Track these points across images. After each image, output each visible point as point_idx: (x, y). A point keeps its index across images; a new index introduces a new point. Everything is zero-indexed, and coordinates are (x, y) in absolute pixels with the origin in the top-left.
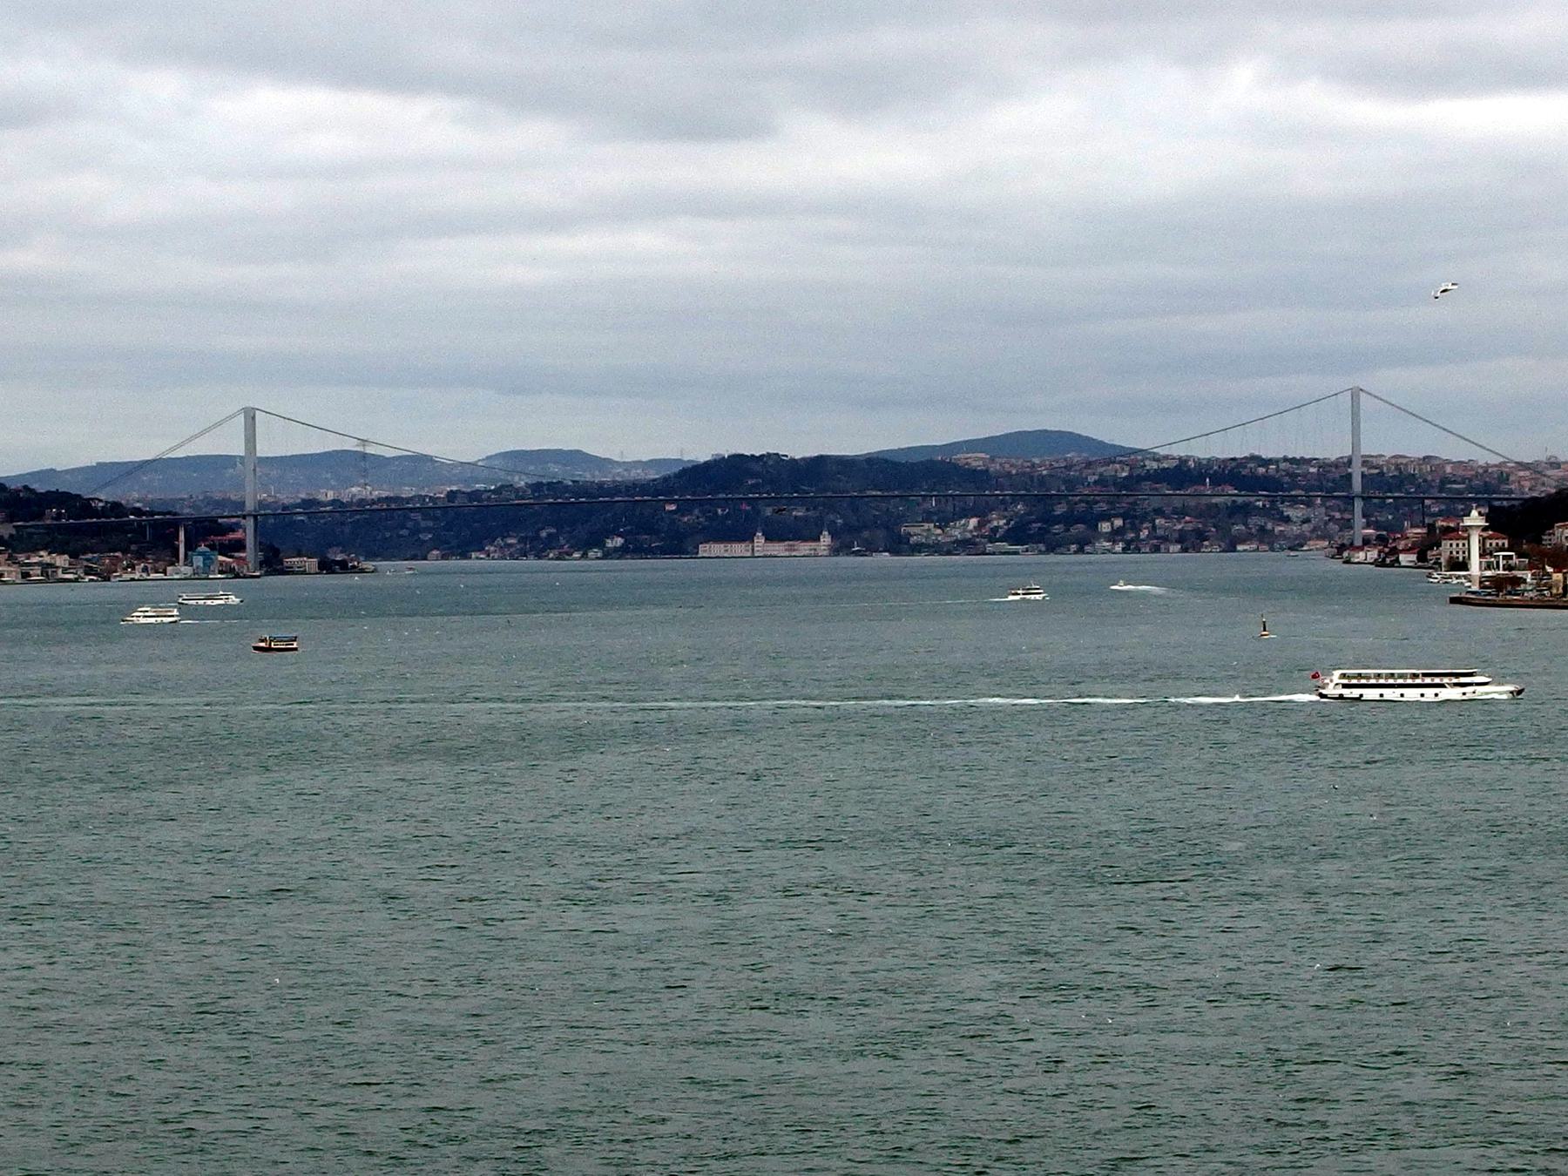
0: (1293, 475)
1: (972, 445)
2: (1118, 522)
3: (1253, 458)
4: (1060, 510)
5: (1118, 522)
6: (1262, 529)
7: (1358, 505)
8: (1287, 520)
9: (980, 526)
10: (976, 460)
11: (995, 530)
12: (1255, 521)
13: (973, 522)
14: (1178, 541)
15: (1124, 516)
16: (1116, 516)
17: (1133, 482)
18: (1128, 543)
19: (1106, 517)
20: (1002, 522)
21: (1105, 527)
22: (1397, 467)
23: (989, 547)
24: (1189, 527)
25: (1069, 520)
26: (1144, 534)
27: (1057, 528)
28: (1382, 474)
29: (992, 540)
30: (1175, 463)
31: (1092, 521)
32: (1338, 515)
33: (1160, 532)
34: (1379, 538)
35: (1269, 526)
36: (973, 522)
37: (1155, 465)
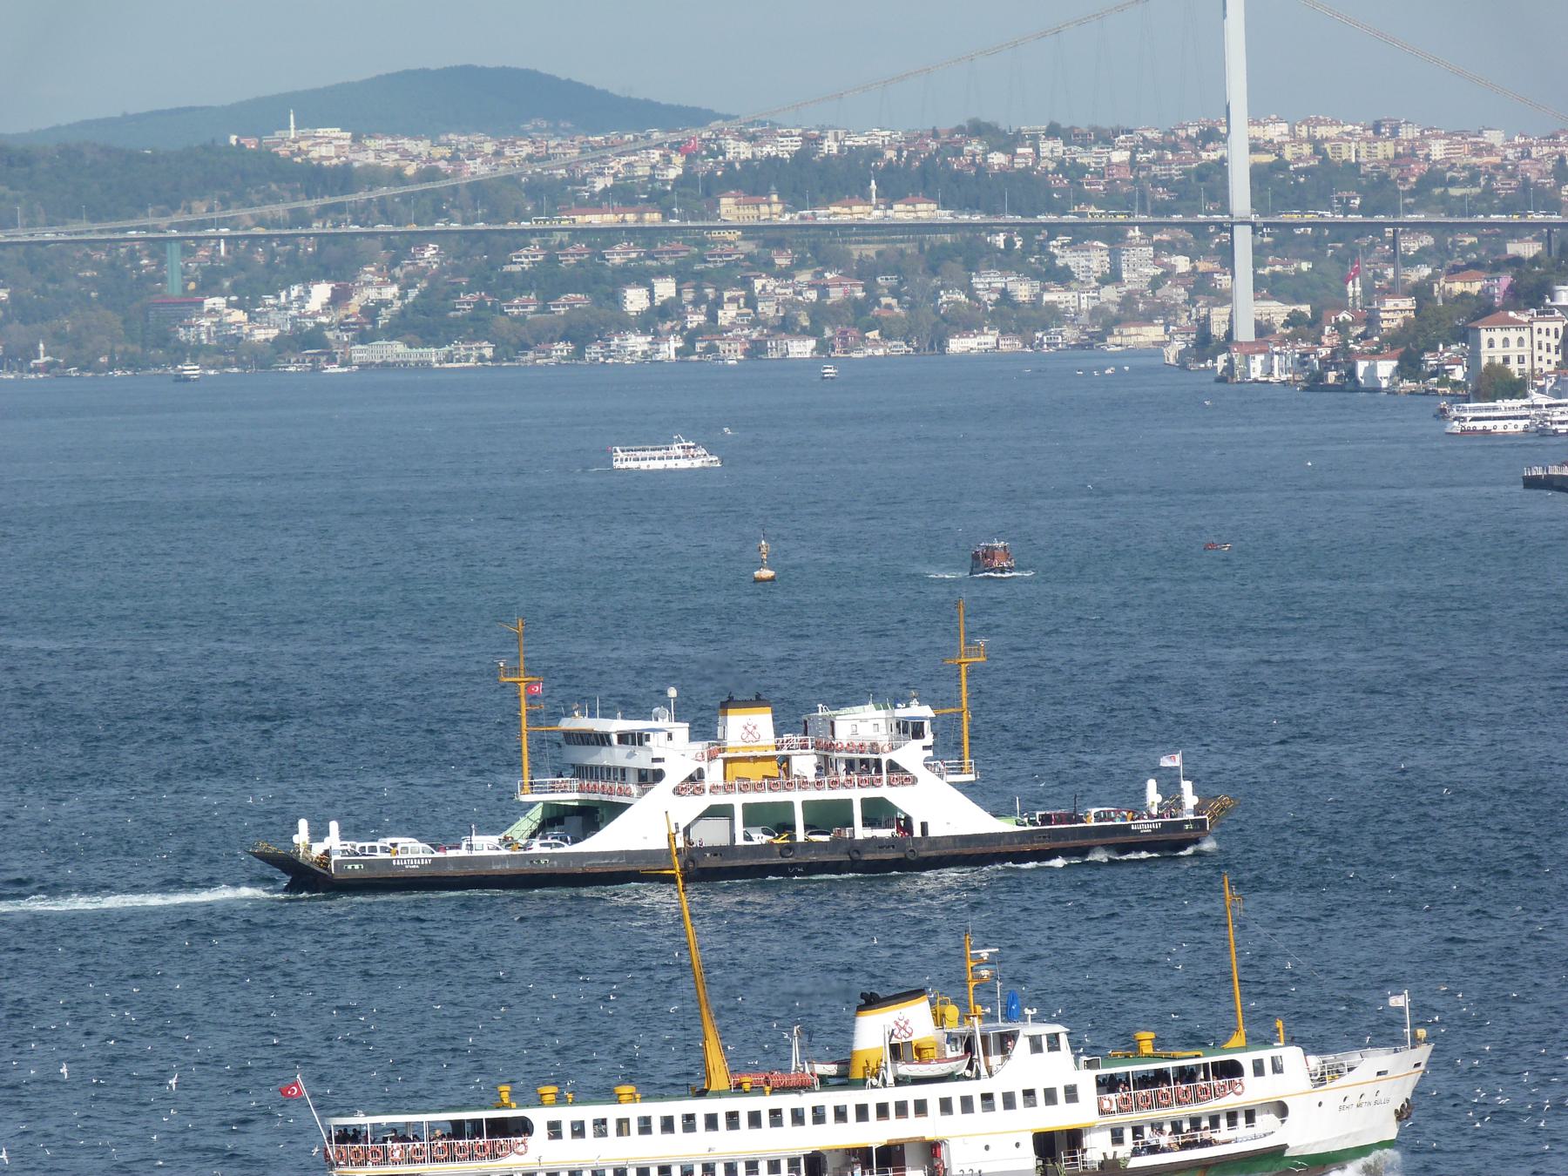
0: (1074, 171)
1: (319, 107)
2: (665, 289)
3: (978, 129)
4: (525, 260)
5: (665, 289)
6: (1004, 293)
7: (1243, 240)
8: (1063, 277)
9: (338, 299)
10: (328, 145)
11: (370, 312)
12: (988, 284)
13: (321, 292)
14: (805, 333)
15: (682, 275)
16: (662, 273)
17: (699, 190)
18: (691, 337)
19: (644, 278)
20: (391, 292)
21: (635, 300)
22: (1317, 145)
23: (360, 353)
24: (836, 294)
25: (548, 281)
26: (727, 314)
27: (524, 306)
28: (1281, 165)
29: (364, 338)
31: (607, 287)
32: (1182, 264)
33: (767, 309)
34: (1293, 320)
35: (1023, 291)
36: (321, 292)
37: (744, 150)
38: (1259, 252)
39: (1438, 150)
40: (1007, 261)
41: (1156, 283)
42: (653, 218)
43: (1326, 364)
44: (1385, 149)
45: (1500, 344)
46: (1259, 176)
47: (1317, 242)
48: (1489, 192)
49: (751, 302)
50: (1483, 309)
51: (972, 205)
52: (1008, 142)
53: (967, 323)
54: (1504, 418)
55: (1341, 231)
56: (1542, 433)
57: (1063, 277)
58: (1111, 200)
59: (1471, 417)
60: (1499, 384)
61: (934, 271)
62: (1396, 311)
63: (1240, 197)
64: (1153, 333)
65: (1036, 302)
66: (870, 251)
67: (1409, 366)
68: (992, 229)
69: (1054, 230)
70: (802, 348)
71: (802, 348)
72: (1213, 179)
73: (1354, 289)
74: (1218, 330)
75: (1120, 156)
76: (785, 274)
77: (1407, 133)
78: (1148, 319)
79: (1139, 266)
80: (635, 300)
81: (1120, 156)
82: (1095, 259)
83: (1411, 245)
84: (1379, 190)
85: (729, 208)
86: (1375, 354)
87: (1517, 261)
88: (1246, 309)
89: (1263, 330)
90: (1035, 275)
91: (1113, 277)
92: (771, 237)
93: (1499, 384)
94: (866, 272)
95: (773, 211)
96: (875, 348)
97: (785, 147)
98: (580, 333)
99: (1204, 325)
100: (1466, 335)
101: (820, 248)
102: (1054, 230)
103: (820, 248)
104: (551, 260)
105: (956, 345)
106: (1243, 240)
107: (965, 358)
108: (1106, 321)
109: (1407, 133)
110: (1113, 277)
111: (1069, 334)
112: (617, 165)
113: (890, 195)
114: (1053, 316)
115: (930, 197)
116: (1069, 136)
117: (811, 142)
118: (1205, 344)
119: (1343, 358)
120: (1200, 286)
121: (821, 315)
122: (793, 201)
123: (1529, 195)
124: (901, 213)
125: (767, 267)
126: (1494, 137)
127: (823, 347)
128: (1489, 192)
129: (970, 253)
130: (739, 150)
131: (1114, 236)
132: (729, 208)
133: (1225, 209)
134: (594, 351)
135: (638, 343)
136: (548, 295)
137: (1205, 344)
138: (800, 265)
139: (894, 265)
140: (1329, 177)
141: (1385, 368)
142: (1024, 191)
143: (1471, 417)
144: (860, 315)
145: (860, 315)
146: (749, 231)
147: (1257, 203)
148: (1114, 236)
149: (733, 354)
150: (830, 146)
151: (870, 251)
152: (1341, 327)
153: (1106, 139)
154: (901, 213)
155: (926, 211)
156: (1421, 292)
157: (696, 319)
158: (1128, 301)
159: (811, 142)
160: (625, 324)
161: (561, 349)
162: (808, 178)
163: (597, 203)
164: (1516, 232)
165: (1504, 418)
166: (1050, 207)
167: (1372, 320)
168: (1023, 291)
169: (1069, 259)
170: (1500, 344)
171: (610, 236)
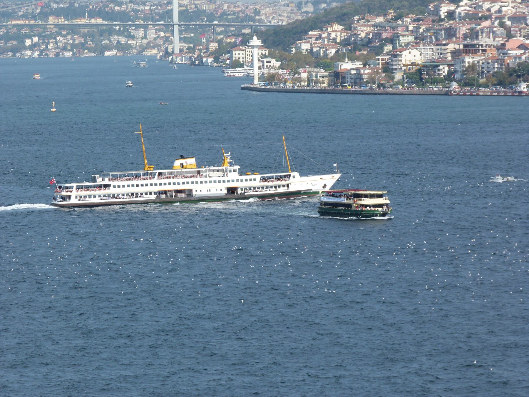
0: (136, 11)
2: (35, 39)
5: (35, 39)
6: (118, 42)
7: (176, 28)
8: (133, 37)
12: (114, 39)
14: (70, 50)
15: (39, 36)
16: (35, 36)
18: (41, 52)
19: (30, 37)
21: (28, 42)
24: (77, 41)
26: (50, 46)
28: (187, 10)
30: (67, 4)
31: (21, 38)
32: (162, 34)
34: (189, 48)
35: (123, 40)
37: (55, 6)
38: (181, 32)
39: (225, 7)
40: (119, 33)
41: (155, 39)
42: (32, 22)
43: (196, 59)
44: (213, 6)
45: (238, 55)
46: (181, 13)
47: (195, 29)
48: (238, 17)
49: (56, 43)
50: (234, 46)
51: (111, 19)
52: (120, 4)
53: (108, 48)
54: (238, 73)
55: (201, 26)
56: (248, 76)
57: (133, 37)
58: (145, 19)
59: (231, 72)
60: (238, 64)
61: (101, 35)
62: (213, 46)
63: (176, 18)
64: (155, 51)
65: (126, 43)
66: (86, 30)
67: (216, 60)
68: (116, 25)
69: (131, 26)
70: (69, 54)
71: (69, 54)
72: (169, 13)
73: (204, 40)
74: (170, 50)
75: (147, 8)
76: (65, 36)
77: (218, 2)
78: (153, 48)
79: (152, 34)
80: (28, 42)
81: (147, 8)
82: (141, 33)
83: (219, 30)
84: (211, 17)
85: (51, 20)
86: (208, 57)
87: (244, 34)
88: (176, 46)
89: (181, 51)
90: (126, 37)
91: (145, 37)
92: (61, 27)
93: (238, 64)
94: (84, 36)
95: (62, 21)
96: (86, 54)
97: (66, 5)
98: (14, 50)
99: (167, 49)
100: (229, 52)
101: (73, 30)
102: (131, 26)
103: (73, 30)
104: (8, 32)
105: (106, 54)
106: (176, 28)
107: (109, 56)
108: (144, 48)
109: (218, 2)
110: (145, 37)
111: (134, 51)
112: (24, 9)
113: (91, 17)
114: (130, 47)
115: (100, 17)
116: (135, 3)
117: (72, 4)
118: (167, 53)
119: (200, 58)
120: (167, 40)
121: (73, 46)
122: (67, 18)
123: (248, 18)
124: (93, 21)
125: (60, 34)
126: (240, 4)
127: (74, 54)
128: (238, 17)
129: (111, 31)
130: (54, 6)
131: (145, 27)
132: (51, 20)
133: (172, 21)
134: (18, 55)
135: (29, 53)
136: (7, 41)
137: (167, 53)
138: (68, 34)
139: (92, 35)
140: (198, 13)
141: (210, 60)
142: (123, 16)
143: (231, 72)
144: (83, 46)
145: (83, 46)
146: (56, 26)
147: (180, 20)
148: (145, 27)
149: (52, 55)
150: (76, 5)
151: (86, 30)
152: (200, 50)
153: (144, 4)
154: (93, 21)
155: (100, 21)
156: (220, 42)
157: (43, 47)
158: (149, 43)
159: (72, 4)
160: (25, 48)
161: (10, 54)
162: (71, 12)
163: (19, 18)
164: (244, 27)
165: (238, 73)
166: (130, 20)
167: (207, 49)
168: (123, 40)
169: (134, 33)
170: (238, 55)
171: (22, 26)
